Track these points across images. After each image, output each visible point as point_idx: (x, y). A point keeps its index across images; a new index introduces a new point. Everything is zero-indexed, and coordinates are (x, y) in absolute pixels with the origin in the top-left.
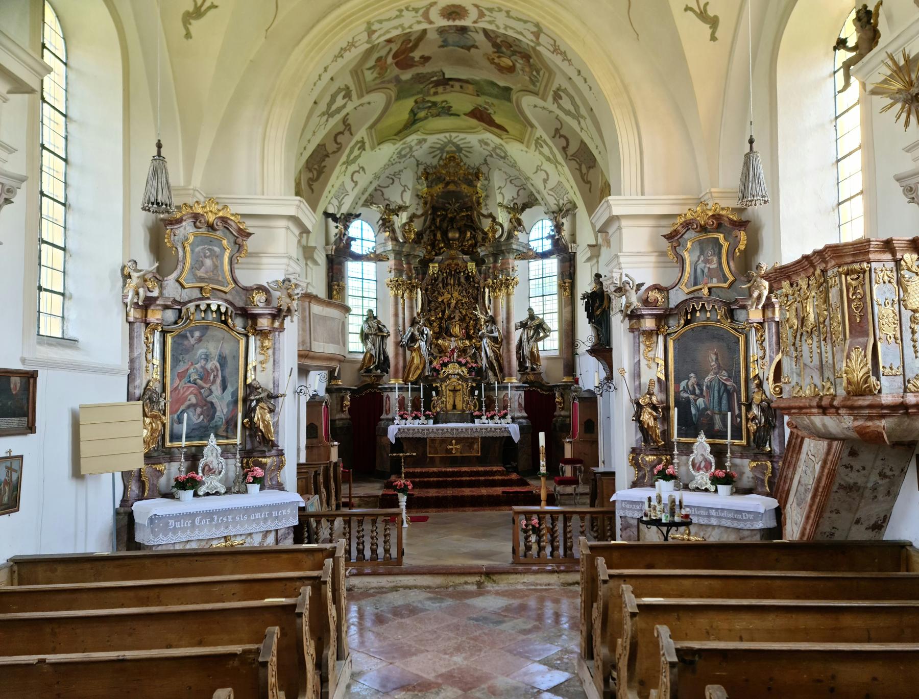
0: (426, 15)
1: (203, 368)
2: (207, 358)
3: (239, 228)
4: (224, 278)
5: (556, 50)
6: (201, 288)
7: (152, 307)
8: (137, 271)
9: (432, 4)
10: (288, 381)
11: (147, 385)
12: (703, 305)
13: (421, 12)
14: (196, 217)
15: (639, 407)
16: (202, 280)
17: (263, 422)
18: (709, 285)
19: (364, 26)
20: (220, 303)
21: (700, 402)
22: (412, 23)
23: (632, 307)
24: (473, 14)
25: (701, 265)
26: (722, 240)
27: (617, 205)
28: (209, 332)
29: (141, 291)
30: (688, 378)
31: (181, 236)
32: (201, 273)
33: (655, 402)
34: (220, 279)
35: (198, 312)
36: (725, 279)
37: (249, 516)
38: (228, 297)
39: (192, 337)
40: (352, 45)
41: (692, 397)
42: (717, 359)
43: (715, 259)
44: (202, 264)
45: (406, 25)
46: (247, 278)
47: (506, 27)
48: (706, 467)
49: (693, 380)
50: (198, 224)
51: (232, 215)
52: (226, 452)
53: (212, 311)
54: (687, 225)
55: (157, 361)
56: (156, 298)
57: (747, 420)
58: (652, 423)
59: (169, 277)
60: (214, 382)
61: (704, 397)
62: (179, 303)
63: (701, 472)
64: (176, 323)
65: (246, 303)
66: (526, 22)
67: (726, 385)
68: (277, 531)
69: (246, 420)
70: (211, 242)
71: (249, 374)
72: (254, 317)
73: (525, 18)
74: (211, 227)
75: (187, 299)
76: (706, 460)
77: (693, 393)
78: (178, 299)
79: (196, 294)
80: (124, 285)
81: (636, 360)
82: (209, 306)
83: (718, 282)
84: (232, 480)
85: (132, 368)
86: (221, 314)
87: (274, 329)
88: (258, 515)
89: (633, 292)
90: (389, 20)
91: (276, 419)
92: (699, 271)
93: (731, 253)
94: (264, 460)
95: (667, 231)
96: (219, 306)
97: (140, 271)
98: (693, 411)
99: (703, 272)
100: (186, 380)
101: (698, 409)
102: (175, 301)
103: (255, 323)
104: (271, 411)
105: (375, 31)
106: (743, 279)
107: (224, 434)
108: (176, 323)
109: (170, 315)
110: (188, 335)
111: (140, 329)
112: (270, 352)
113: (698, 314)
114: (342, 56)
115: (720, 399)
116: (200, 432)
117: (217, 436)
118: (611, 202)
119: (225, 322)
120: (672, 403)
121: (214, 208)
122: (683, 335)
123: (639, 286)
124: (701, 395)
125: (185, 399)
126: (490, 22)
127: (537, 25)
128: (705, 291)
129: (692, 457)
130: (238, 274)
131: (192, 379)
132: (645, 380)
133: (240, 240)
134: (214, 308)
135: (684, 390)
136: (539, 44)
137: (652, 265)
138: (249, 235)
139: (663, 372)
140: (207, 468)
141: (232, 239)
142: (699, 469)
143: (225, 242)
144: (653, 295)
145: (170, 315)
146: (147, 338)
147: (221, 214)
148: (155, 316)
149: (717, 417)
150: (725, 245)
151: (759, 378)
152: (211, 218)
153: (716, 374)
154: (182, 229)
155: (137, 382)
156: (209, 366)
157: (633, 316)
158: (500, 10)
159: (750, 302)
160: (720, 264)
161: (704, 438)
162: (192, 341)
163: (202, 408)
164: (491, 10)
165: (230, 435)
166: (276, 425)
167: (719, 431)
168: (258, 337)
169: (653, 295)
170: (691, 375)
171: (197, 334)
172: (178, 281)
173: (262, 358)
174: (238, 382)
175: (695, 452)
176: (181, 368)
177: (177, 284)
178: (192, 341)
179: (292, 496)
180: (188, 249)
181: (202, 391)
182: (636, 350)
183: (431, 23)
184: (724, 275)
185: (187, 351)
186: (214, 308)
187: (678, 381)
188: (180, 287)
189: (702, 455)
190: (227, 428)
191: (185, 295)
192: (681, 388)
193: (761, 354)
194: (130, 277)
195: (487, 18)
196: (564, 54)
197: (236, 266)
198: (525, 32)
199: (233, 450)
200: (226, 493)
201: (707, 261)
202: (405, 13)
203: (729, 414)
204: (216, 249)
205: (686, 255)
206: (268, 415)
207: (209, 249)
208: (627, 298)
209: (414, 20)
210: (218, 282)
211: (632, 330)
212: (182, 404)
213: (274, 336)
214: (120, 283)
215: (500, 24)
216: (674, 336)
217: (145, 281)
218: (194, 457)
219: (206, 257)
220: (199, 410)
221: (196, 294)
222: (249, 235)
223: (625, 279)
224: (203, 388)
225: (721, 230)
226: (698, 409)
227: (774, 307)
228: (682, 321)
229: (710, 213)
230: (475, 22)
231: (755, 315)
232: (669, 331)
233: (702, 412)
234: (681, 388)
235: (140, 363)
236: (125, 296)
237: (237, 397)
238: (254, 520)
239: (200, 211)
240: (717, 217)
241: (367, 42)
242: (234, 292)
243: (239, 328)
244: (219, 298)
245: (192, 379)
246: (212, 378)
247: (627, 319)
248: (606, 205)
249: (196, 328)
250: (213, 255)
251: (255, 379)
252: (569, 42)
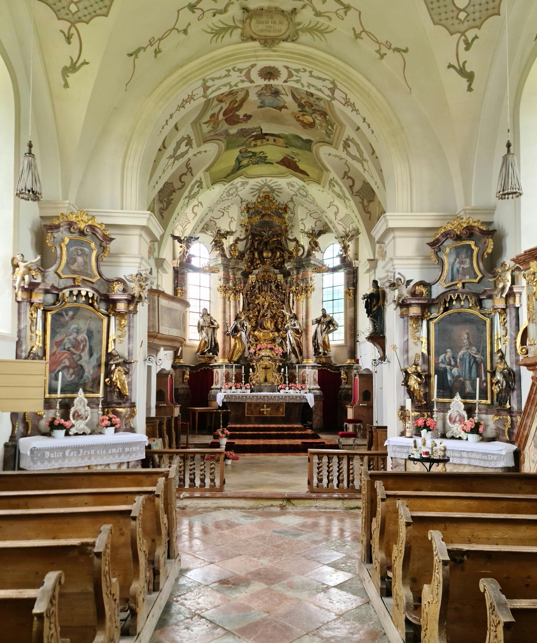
0: (248, 75)
1: (75, 339)
2: (78, 332)
3: (104, 234)
4: (92, 271)
6: (74, 279)
7: (36, 291)
8: (24, 261)
9: (253, 66)
10: (140, 352)
11: (31, 350)
12: (458, 295)
13: (244, 72)
14: (71, 224)
15: (407, 375)
16: (74, 272)
17: (120, 381)
18: (463, 281)
19: (201, 82)
20: (88, 290)
21: (455, 371)
23: (403, 298)
24: (284, 74)
25: (457, 266)
26: (473, 247)
27: (392, 219)
28: (80, 313)
29: (27, 277)
30: (446, 353)
31: (59, 239)
32: (74, 267)
33: (420, 371)
34: (89, 272)
35: (72, 296)
36: (476, 276)
37: (107, 451)
38: (95, 286)
39: (67, 315)
40: (191, 98)
41: (448, 367)
42: (468, 338)
43: (468, 260)
44: (75, 261)
45: (233, 84)
46: (109, 273)
47: (309, 85)
48: (460, 421)
49: (449, 353)
50: (72, 229)
51: (99, 224)
52: (92, 403)
53: (82, 296)
54: (447, 235)
55: (39, 332)
56: (38, 284)
57: (492, 384)
58: (417, 387)
59: (50, 270)
60: (83, 350)
61: (458, 367)
62: (57, 289)
63: (456, 424)
64: (54, 304)
65: (108, 291)
66: (324, 80)
67: (475, 358)
68: (128, 463)
69: (107, 380)
70: (82, 243)
71: (110, 345)
72: (115, 302)
74: (82, 233)
75: (63, 286)
76: (460, 415)
77: (449, 364)
78: (56, 285)
79: (70, 282)
80: (14, 272)
81: (405, 339)
82: (79, 292)
83: (470, 278)
84: (96, 424)
85: (19, 336)
86: (89, 298)
87: (129, 312)
88: (114, 450)
89: (404, 286)
90: (220, 78)
91: (130, 380)
92: (455, 270)
93: (481, 256)
94: (120, 410)
95: (431, 240)
96: (87, 292)
97: (26, 262)
98: (449, 378)
99: (458, 271)
100: (62, 347)
101: (453, 376)
102: (53, 287)
103: (115, 306)
104: (126, 373)
105: (209, 87)
106: (490, 275)
107: (91, 390)
108: (54, 304)
109: (50, 298)
110: (64, 313)
111: (25, 306)
112: (126, 329)
113: (454, 303)
114: (183, 107)
115: (470, 368)
116: (71, 388)
117: (85, 391)
118: (388, 218)
119: (92, 305)
120: (433, 372)
121: (85, 218)
122: (442, 320)
123: (409, 282)
124: (456, 365)
125: (61, 362)
126: (297, 81)
128: (460, 286)
129: (449, 412)
130: (103, 269)
131: (66, 347)
132: (412, 354)
133: (104, 244)
134: (83, 293)
135: (442, 362)
136: (334, 98)
137: (418, 266)
138: (112, 239)
139: (426, 348)
140: (76, 414)
141: (98, 243)
142: (454, 422)
143: (93, 245)
144: (420, 289)
145: (50, 298)
146: (32, 315)
147: (90, 223)
148: (38, 298)
149: (468, 383)
150: (476, 249)
151: (502, 352)
152: (82, 226)
153: (468, 349)
154: (60, 233)
155: (24, 348)
156: (80, 338)
157: (403, 305)
158: (305, 71)
159: (496, 293)
160: (472, 264)
161: (460, 399)
162: (67, 318)
163: (74, 368)
164: (297, 71)
165: (94, 390)
166: (130, 384)
167: (469, 393)
168: (117, 318)
169: (420, 289)
170: (448, 350)
171: (71, 313)
172: (56, 273)
173: (119, 333)
174: (101, 351)
175: (452, 409)
176: (58, 338)
177: (56, 275)
178: (67, 318)
179: (141, 436)
180: (64, 249)
181: (74, 356)
182: (406, 331)
183: (252, 82)
184: (475, 273)
185: (63, 326)
186: (83, 293)
187: (437, 354)
188: (58, 278)
189: (458, 411)
190: (93, 385)
191: (62, 284)
192: (440, 361)
193: (504, 333)
194: (18, 266)
195: (295, 78)
197: (101, 263)
199: (97, 402)
200: (91, 434)
201: (462, 262)
202: (232, 73)
203: (478, 379)
204: (86, 249)
205: (445, 258)
206: (124, 376)
207: (81, 250)
208: (399, 291)
209: (239, 79)
210: (87, 275)
211: (402, 316)
212: (59, 365)
213: (130, 316)
214: (11, 271)
216: (435, 321)
217: (30, 270)
218: (66, 406)
219: (78, 255)
220: (71, 371)
221: (70, 282)
222: (112, 239)
223: (397, 276)
224: (75, 354)
225: (473, 238)
226: (453, 376)
227: (515, 297)
228: (442, 309)
229: (465, 225)
230: (286, 81)
231: (500, 304)
232: (431, 317)
233: (456, 378)
234: (440, 361)
235: (26, 333)
236: (14, 281)
237: (101, 362)
238: (111, 454)
239: (73, 219)
240: (470, 228)
241: (204, 96)
242: (99, 283)
243: (103, 310)
244: (87, 286)
245: (66, 347)
246: (81, 346)
247: (398, 308)
248: (383, 220)
249: (71, 309)
250: (83, 254)
251: (114, 349)
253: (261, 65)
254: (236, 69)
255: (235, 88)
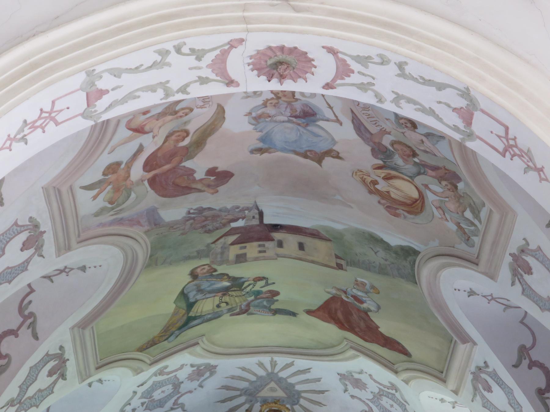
0: (220, 65)
5: (510, 148)
13: (209, 58)
19: (82, 77)
22: (185, 79)
24: (325, 67)
40: (49, 116)
45: (175, 85)
47: (398, 98)
66: (441, 87)
73: (439, 79)
90: (137, 70)
105: (102, 93)
114: (24, 139)
126: (363, 87)
127: (466, 93)
136: (471, 136)
158: (384, 61)
164: (364, 60)
183: (230, 82)
195: (355, 78)
196: (525, 155)
198: (437, 108)
202: (173, 57)
215: (386, 92)
230: (328, 86)
241: (85, 115)
252: (538, 130)
253: (258, 42)
254: (185, 50)
255: (179, 97)
